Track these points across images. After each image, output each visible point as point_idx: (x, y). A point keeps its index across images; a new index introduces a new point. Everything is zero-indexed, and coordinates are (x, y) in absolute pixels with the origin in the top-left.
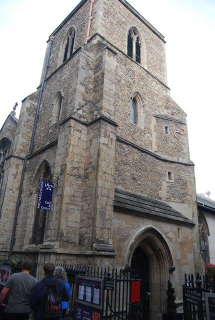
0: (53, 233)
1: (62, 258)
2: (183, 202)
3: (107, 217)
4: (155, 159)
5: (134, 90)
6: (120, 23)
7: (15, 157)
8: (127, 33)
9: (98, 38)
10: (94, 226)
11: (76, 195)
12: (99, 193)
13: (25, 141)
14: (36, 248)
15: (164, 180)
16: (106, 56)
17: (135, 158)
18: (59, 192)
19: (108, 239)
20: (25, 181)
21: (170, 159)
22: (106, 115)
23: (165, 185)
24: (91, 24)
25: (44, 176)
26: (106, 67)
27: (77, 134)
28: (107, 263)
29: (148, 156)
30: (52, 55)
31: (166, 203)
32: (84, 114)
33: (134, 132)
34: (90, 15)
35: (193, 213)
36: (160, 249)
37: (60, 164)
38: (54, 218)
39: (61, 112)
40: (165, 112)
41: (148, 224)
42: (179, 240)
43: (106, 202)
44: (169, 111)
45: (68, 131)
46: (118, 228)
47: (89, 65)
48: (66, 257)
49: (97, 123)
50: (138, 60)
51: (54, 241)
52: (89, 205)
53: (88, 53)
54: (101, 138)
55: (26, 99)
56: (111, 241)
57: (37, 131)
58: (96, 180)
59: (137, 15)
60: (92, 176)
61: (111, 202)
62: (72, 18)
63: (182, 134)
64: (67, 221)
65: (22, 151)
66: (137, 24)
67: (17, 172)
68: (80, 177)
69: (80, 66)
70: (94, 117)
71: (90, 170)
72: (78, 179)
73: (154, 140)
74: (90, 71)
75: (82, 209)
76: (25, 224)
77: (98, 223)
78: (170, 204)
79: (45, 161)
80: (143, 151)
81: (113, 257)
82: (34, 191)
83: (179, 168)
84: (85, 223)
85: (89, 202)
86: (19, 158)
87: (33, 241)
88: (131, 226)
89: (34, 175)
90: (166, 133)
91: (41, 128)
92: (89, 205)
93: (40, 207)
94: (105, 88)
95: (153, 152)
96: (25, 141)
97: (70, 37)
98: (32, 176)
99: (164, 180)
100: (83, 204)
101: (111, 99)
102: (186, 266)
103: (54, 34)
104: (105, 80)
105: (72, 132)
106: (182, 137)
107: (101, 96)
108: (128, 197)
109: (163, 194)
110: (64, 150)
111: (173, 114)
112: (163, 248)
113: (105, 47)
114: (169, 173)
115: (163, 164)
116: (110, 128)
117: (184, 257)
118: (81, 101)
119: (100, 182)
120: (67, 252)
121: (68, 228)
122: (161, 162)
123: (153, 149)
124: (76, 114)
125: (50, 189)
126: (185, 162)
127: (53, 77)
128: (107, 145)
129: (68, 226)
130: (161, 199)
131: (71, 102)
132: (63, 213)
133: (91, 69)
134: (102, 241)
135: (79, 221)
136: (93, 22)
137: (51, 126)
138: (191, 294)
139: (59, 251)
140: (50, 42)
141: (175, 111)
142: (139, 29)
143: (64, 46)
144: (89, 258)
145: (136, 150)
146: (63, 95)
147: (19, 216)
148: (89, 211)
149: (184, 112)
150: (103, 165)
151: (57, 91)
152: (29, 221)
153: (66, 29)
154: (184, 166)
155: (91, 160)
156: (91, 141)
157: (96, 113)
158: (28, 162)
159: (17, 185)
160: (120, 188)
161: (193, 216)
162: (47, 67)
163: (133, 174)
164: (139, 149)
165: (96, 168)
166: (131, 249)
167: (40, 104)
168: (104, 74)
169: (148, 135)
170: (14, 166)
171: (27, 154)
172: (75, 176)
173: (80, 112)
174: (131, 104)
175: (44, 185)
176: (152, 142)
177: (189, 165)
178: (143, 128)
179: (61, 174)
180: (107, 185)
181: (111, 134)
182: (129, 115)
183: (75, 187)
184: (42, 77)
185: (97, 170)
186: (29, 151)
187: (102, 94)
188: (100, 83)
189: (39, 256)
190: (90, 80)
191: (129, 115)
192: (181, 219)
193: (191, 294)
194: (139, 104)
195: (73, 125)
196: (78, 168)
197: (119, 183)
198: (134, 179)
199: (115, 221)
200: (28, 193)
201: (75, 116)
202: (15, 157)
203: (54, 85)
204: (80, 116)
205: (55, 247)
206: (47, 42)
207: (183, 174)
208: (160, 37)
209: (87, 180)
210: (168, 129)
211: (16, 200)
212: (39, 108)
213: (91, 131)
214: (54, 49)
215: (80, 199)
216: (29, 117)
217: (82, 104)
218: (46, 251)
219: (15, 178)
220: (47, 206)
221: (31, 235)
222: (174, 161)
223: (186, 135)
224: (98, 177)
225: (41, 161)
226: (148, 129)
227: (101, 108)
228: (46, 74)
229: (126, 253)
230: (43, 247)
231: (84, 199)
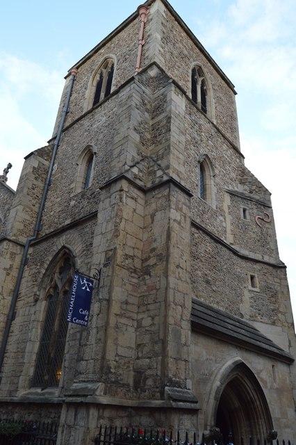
0: (91, 366)
1: (107, 413)
2: (274, 323)
3: (183, 340)
4: (232, 255)
5: (202, 151)
6: (183, 57)
7: (10, 241)
8: (190, 71)
9: (153, 72)
11: (130, 301)
12: (171, 298)
13: (28, 218)
14: (43, 394)
16: (173, 92)
17: (207, 250)
18: (103, 294)
19: (186, 379)
20: (23, 280)
21: (252, 255)
22: (175, 177)
23: (247, 295)
24: (142, 51)
25: (60, 273)
26: (173, 108)
27: (131, 202)
29: (224, 249)
30: (74, 95)
31: (250, 323)
32: (141, 174)
33: (204, 212)
34: (141, 38)
35: (289, 341)
36: (251, 398)
37: (103, 248)
38: (92, 339)
39: (92, 176)
40: (239, 188)
41: (233, 357)
42: (276, 386)
43: (180, 317)
44: (246, 187)
45: (118, 197)
46: (196, 361)
48: (114, 413)
49: (162, 189)
50: (204, 110)
51: (92, 381)
52: (153, 318)
53: (143, 88)
55: (32, 154)
56: (189, 383)
57: (48, 204)
58: (167, 277)
59: (202, 50)
60: (158, 270)
62: (108, 45)
63: (267, 219)
64: (117, 345)
65: (21, 232)
66: (201, 61)
67: (11, 266)
68: (135, 271)
70: (157, 181)
71: (152, 261)
72: (133, 275)
73: (229, 227)
75: (139, 326)
76: (21, 352)
79: (64, 247)
80: (218, 241)
81: (194, 412)
82: (41, 297)
83: (265, 271)
84: (146, 349)
85: (152, 313)
86: (16, 243)
87: (37, 381)
88: (214, 359)
89: (44, 271)
90: (245, 217)
91: (55, 202)
92: (153, 318)
93: (72, 318)
95: (228, 244)
96: (28, 218)
97: (104, 71)
98: (39, 273)
100: (140, 316)
101: (181, 156)
102: (287, 430)
103: (78, 66)
104: (173, 128)
105: (124, 199)
106: (267, 225)
107: (166, 150)
108: (206, 311)
109: (246, 308)
110: (111, 226)
111: (251, 192)
112: (256, 397)
113: (171, 81)
114: (252, 277)
115: (243, 263)
117: (284, 414)
118: (135, 155)
119: (172, 280)
120: (116, 401)
121: (117, 358)
123: (229, 239)
124: (130, 173)
125: (88, 290)
126: (272, 261)
127: (76, 126)
128: (179, 223)
129: (117, 355)
130: (242, 316)
131: (119, 155)
132: (111, 331)
133: (147, 111)
134: (177, 382)
135: (134, 346)
136: (146, 48)
137: (75, 196)
139: (104, 400)
140: (71, 77)
141: (254, 187)
142: (205, 70)
143: (95, 83)
144: (157, 415)
145: (207, 238)
146: (95, 149)
147: (10, 339)
148: (153, 328)
149: (267, 190)
150: (175, 253)
151: (85, 145)
152: (29, 347)
153: (99, 59)
155: (154, 245)
156: (153, 216)
157: (159, 173)
158: (31, 250)
159: (10, 286)
161: (290, 346)
162: (65, 111)
163: (206, 275)
165: (165, 257)
166: (216, 399)
167: (53, 165)
168: (170, 118)
169: (221, 218)
170: (9, 255)
171: (30, 239)
172: (128, 269)
173: (135, 170)
174: (198, 170)
175: (79, 282)
176: (226, 227)
177: (281, 267)
178: (215, 208)
179: (105, 265)
180: (183, 286)
182: (197, 185)
183: (130, 288)
184: (57, 126)
185: (167, 261)
186: (32, 234)
187: (169, 146)
189: (64, 411)
191: (197, 185)
192: (276, 350)
194: (208, 173)
195: (125, 189)
196: (132, 257)
198: (208, 282)
199: (192, 347)
200: (32, 299)
201: (129, 176)
202: (10, 241)
203: (79, 138)
204: (136, 177)
205: (98, 393)
206: (65, 78)
207: (270, 280)
208: (230, 85)
209: (147, 277)
210: (247, 212)
211: (6, 311)
212: (52, 170)
213: (153, 200)
214: (77, 87)
215: (135, 309)
216: (35, 182)
217: (136, 160)
218: (79, 400)
219: (8, 274)
220: (82, 317)
221: (32, 371)
222: (257, 259)
223: (272, 222)
224: (170, 273)
225: (56, 248)
226: (220, 210)
227: (168, 167)
228: (64, 122)
229: (209, 406)
230: (71, 393)
231: (144, 308)
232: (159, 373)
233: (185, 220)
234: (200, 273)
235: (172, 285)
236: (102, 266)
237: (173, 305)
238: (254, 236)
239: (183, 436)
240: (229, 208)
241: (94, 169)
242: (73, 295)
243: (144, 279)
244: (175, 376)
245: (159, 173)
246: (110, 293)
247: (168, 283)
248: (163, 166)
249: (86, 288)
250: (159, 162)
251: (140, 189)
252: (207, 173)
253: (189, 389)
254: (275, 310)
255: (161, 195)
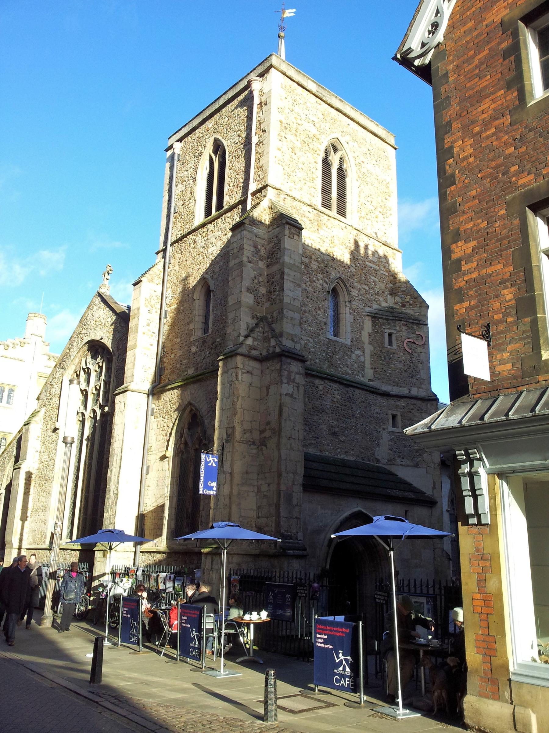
2: (416, 465)
3: (295, 501)
10: (278, 516)
12: (283, 468)
15: (384, 429)
17: (335, 400)
19: (297, 532)
21: (395, 390)
22: (288, 343)
26: (287, 259)
28: (296, 565)
29: (357, 391)
32: (256, 343)
33: (334, 353)
44: (398, 299)
45: (234, 374)
47: (258, 251)
50: (342, 211)
54: (284, 386)
56: (300, 536)
58: (279, 450)
60: (272, 443)
61: (300, 479)
68: (254, 443)
69: (245, 259)
70: (271, 350)
71: (267, 434)
72: (252, 446)
73: (368, 360)
74: (260, 262)
75: (259, 491)
77: (283, 513)
78: (393, 469)
83: (411, 407)
90: (390, 344)
92: (269, 485)
94: (286, 300)
99: (384, 429)
104: (287, 285)
106: (419, 349)
107: (279, 313)
111: (404, 306)
114: (394, 417)
115: (384, 401)
116: (295, 367)
119: (283, 452)
121: (241, 519)
122: (379, 398)
124: (244, 346)
126: (422, 393)
128: (291, 396)
129: (241, 516)
130: (378, 461)
131: (233, 323)
138: (379, 595)
145: (336, 386)
149: (424, 301)
154: (420, 402)
156: (268, 388)
160: (311, 450)
161: (434, 488)
163: (332, 427)
164: (341, 383)
165: (278, 432)
168: (283, 274)
169: (358, 352)
173: (250, 341)
174: (329, 304)
175: (206, 460)
177: (432, 400)
178: (349, 343)
179: (227, 441)
181: (297, 376)
187: (282, 309)
188: (277, 288)
190: (261, 279)
191: (325, 324)
192: (411, 495)
193: (379, 595)
194: (343, 297)
195: (240, 366)
197: (311, 444)
198: (334, 434)
204: (251, 348)
209: (264, 448)
213: (268, 371)
217: (251, 326)
222: (401, 394)
226: (357, 343)
227: (281, 335)
232: (273, 529)
233: (298, 390)
234: (324, 427)
235: (283, 457)
236: (224, 441)
237: (284, 474)
238: (400, 366)
239: (290, 574)
240: (370, 336)
241: (213, 311)
242: (202, 472)
243: (262, 449)
244: (287, 531)
245: (273, 342)
246: (232, 467)
247: (280, 456)
248: (277, 331)
249: (212, 463)
250: (274, 326)
251: (255, 359)
252: (341, 299)
253: (301, 540)
254: (420, 450)
255: (274, 368)
